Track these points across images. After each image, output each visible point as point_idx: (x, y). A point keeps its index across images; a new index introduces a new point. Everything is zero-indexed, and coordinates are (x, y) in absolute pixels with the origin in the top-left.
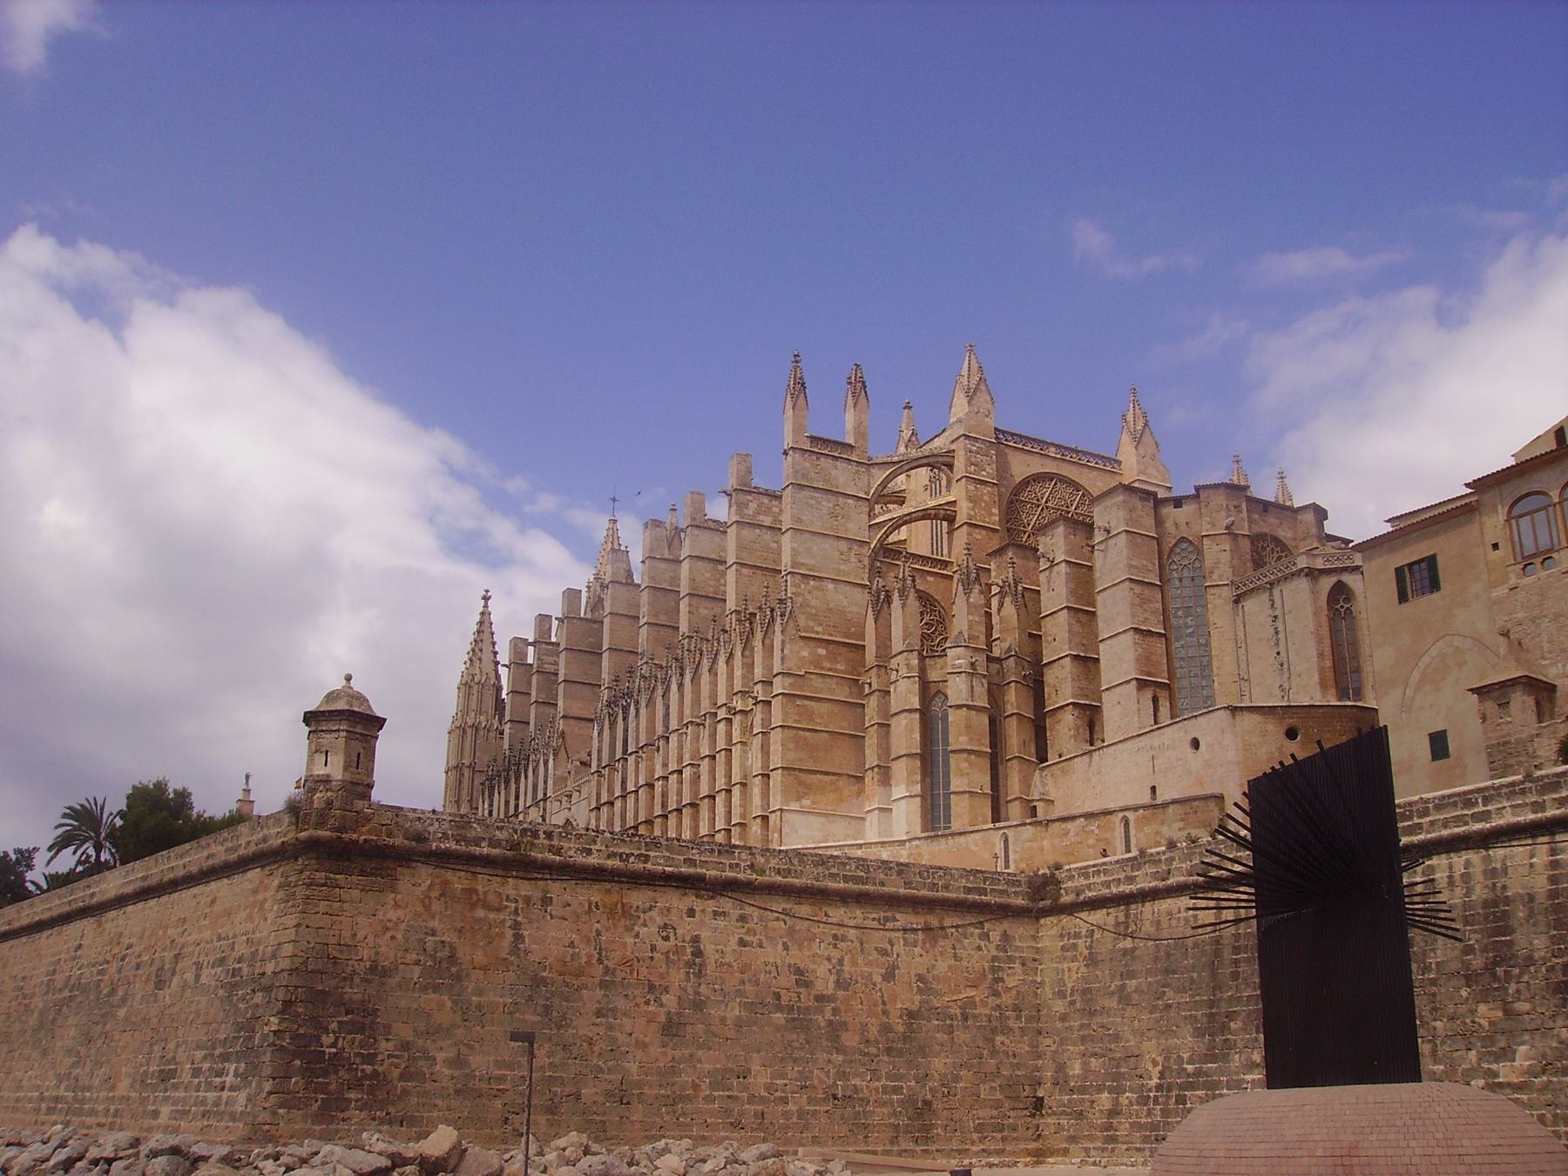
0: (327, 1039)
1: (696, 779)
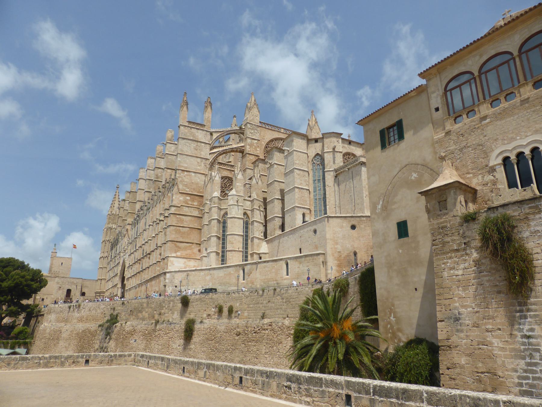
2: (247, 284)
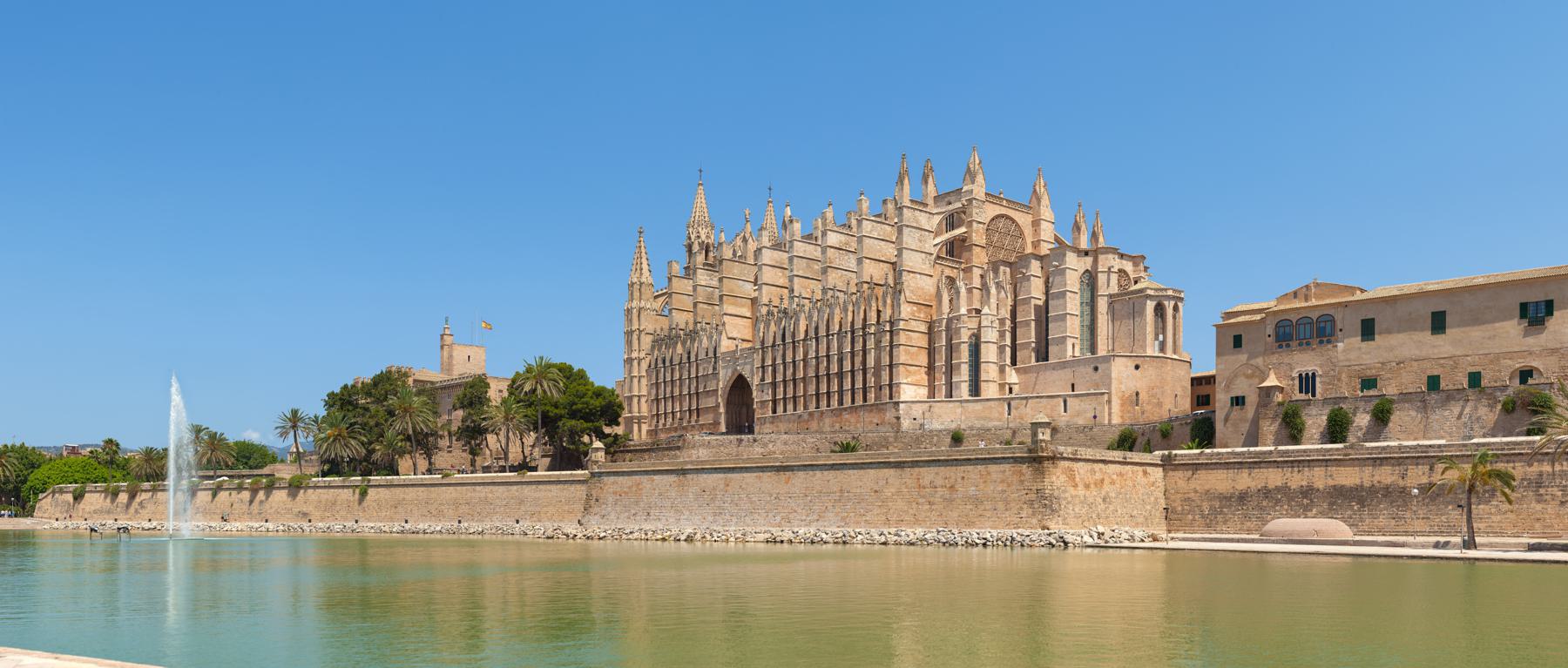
1: (841, 361)
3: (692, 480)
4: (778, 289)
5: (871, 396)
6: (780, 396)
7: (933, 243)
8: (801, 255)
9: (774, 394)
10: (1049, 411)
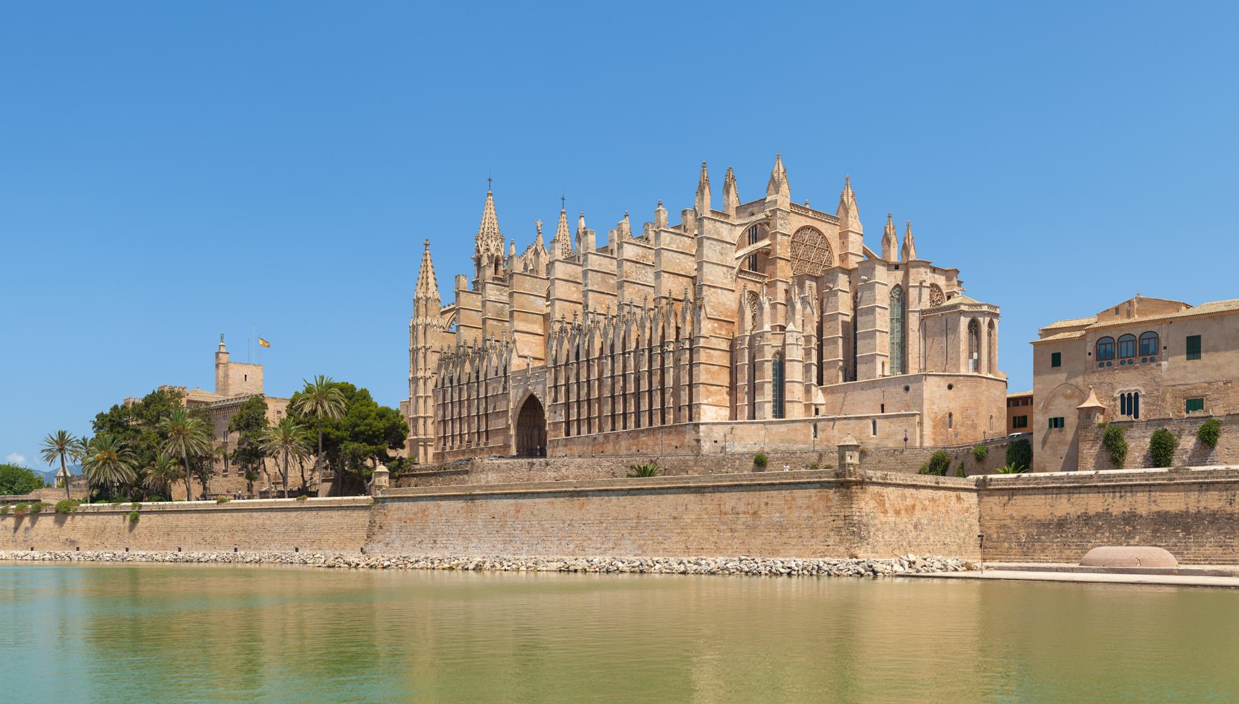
0: (862, 533)
1: (637, 380)
2: (821, 441)
3: (481, 505)
4: (572, 304)
5: (670, 417)
6: (574, 417)
7: (735, 257)
8: (596, 269)
9: (568, 415)
10: (857, 433)
